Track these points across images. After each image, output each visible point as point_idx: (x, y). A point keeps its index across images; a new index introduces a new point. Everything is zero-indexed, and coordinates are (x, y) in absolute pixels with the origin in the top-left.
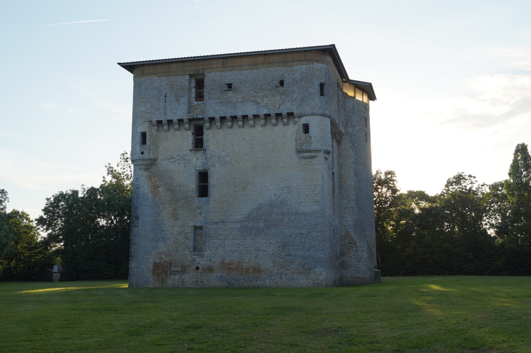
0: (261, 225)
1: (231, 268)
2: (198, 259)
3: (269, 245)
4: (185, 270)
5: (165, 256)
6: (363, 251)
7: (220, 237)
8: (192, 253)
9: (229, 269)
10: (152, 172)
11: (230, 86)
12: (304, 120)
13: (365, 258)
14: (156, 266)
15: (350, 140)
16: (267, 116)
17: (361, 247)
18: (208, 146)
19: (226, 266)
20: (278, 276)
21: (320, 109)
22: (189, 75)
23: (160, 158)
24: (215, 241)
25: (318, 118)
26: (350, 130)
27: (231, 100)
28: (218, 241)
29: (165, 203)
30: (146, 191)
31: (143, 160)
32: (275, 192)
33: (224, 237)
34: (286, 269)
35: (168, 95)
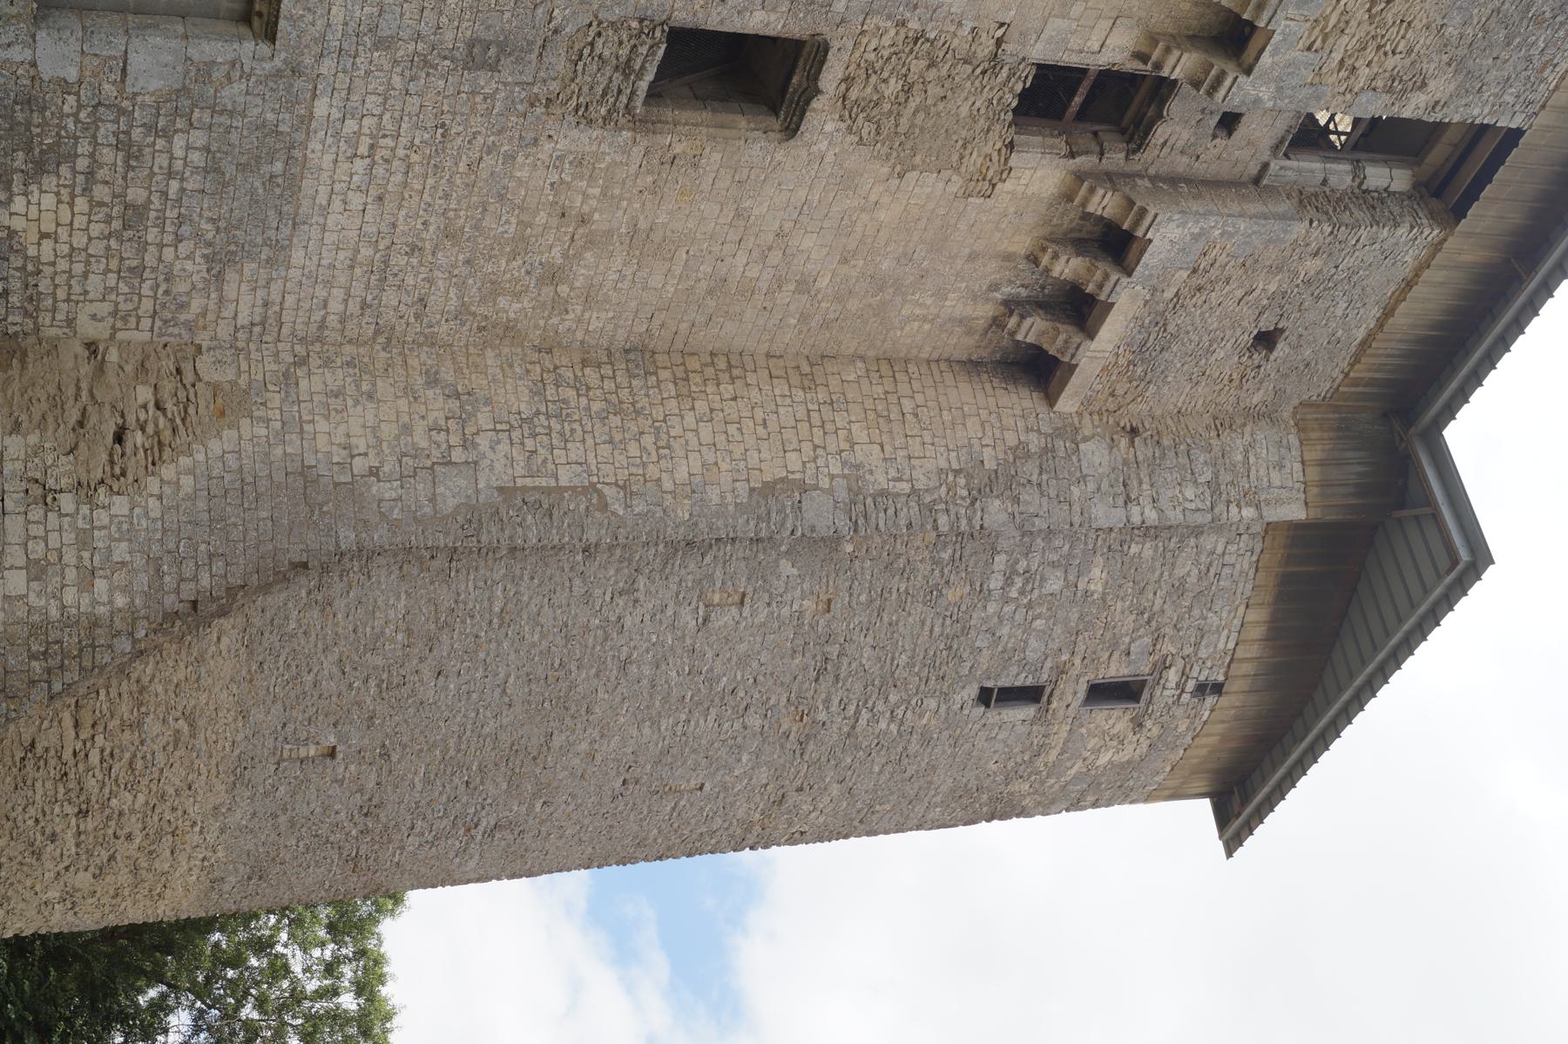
6: (36, 570)
15: (1021, 452)
17: (84, 540)
26: (1095, 455)
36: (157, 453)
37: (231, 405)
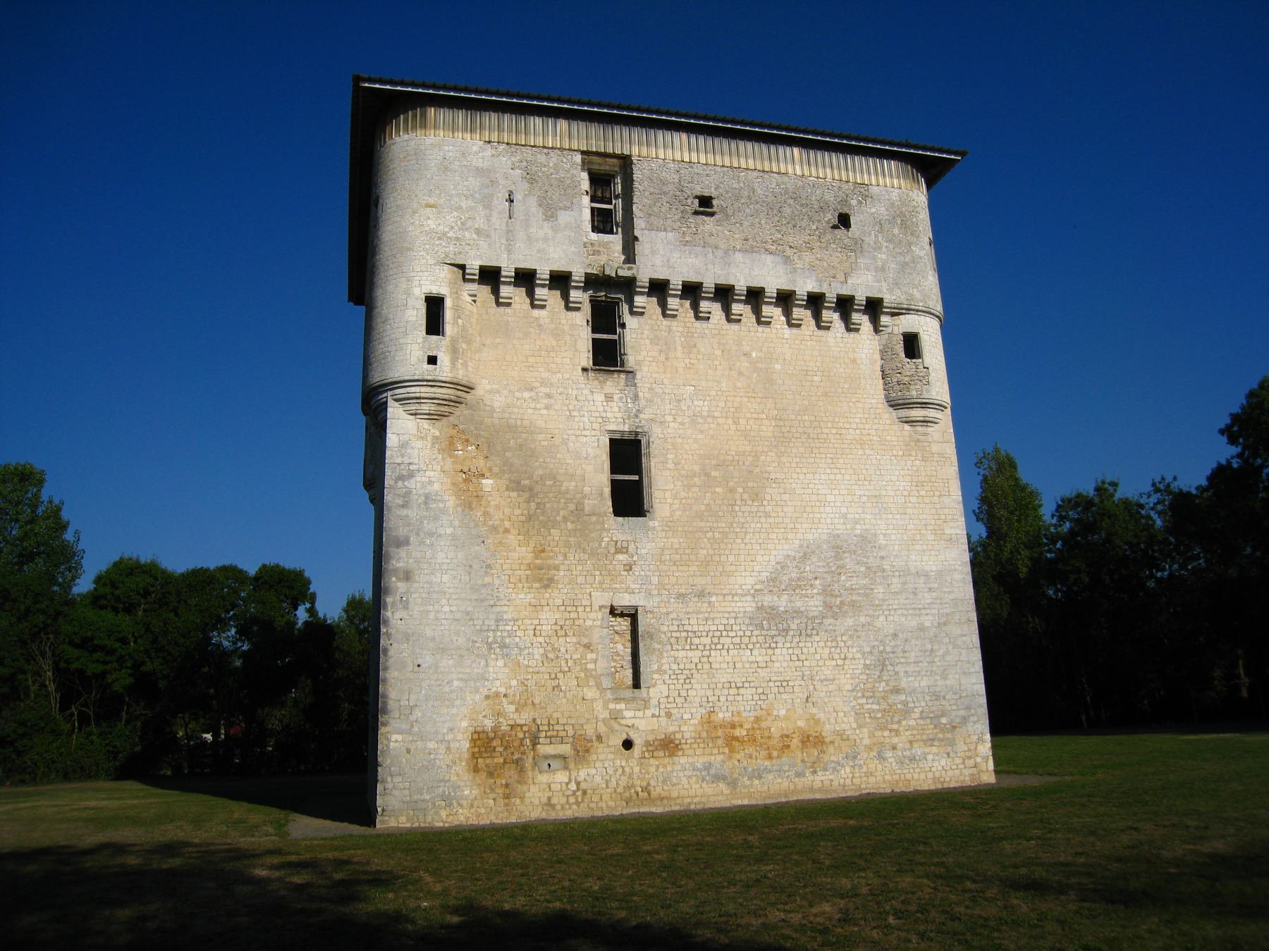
0: (814, 605)
1: (736, 739)
2: (628, 714)
3: (840, 662)
4: (587, 751)
5: (512, 708)
7: (696, 641)
8: (609, 695)
9: (731, 741)
10: (455, 426)
11: (705, 202)
14: (483, 743)
16: (815, 302)
18: (639, 363)
20: (872, 754)
24: (682, 654)
28: (690, 654)
29: (507, 531)
30: (436, 486)
31: (432, 383)
32: (844, 510)
33: (707, 641)
34: (891, 731)
35: (518, 197)
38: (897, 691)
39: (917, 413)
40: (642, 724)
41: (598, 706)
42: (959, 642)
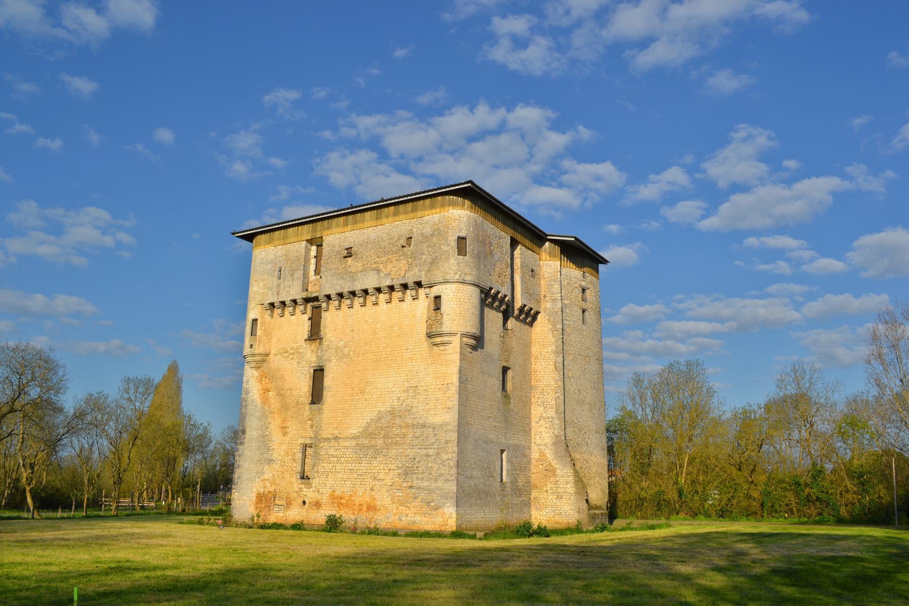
2: (305, 490)
6: (567, 483)
8: (300, 481)
12: (435, 291)
13: (571, 494)
16: (392, 288)
19: (336, 500)
21: (456, 274)
22: (307, 241)
23: (273, 352)
25: (454, 287)
27: (350, 269)
36: (550, 464)
37: (542, 454)
38: (411, 487)
39: (438, 340)
40: (309, 495)
41: (295, 485)
42: (446, 463)
